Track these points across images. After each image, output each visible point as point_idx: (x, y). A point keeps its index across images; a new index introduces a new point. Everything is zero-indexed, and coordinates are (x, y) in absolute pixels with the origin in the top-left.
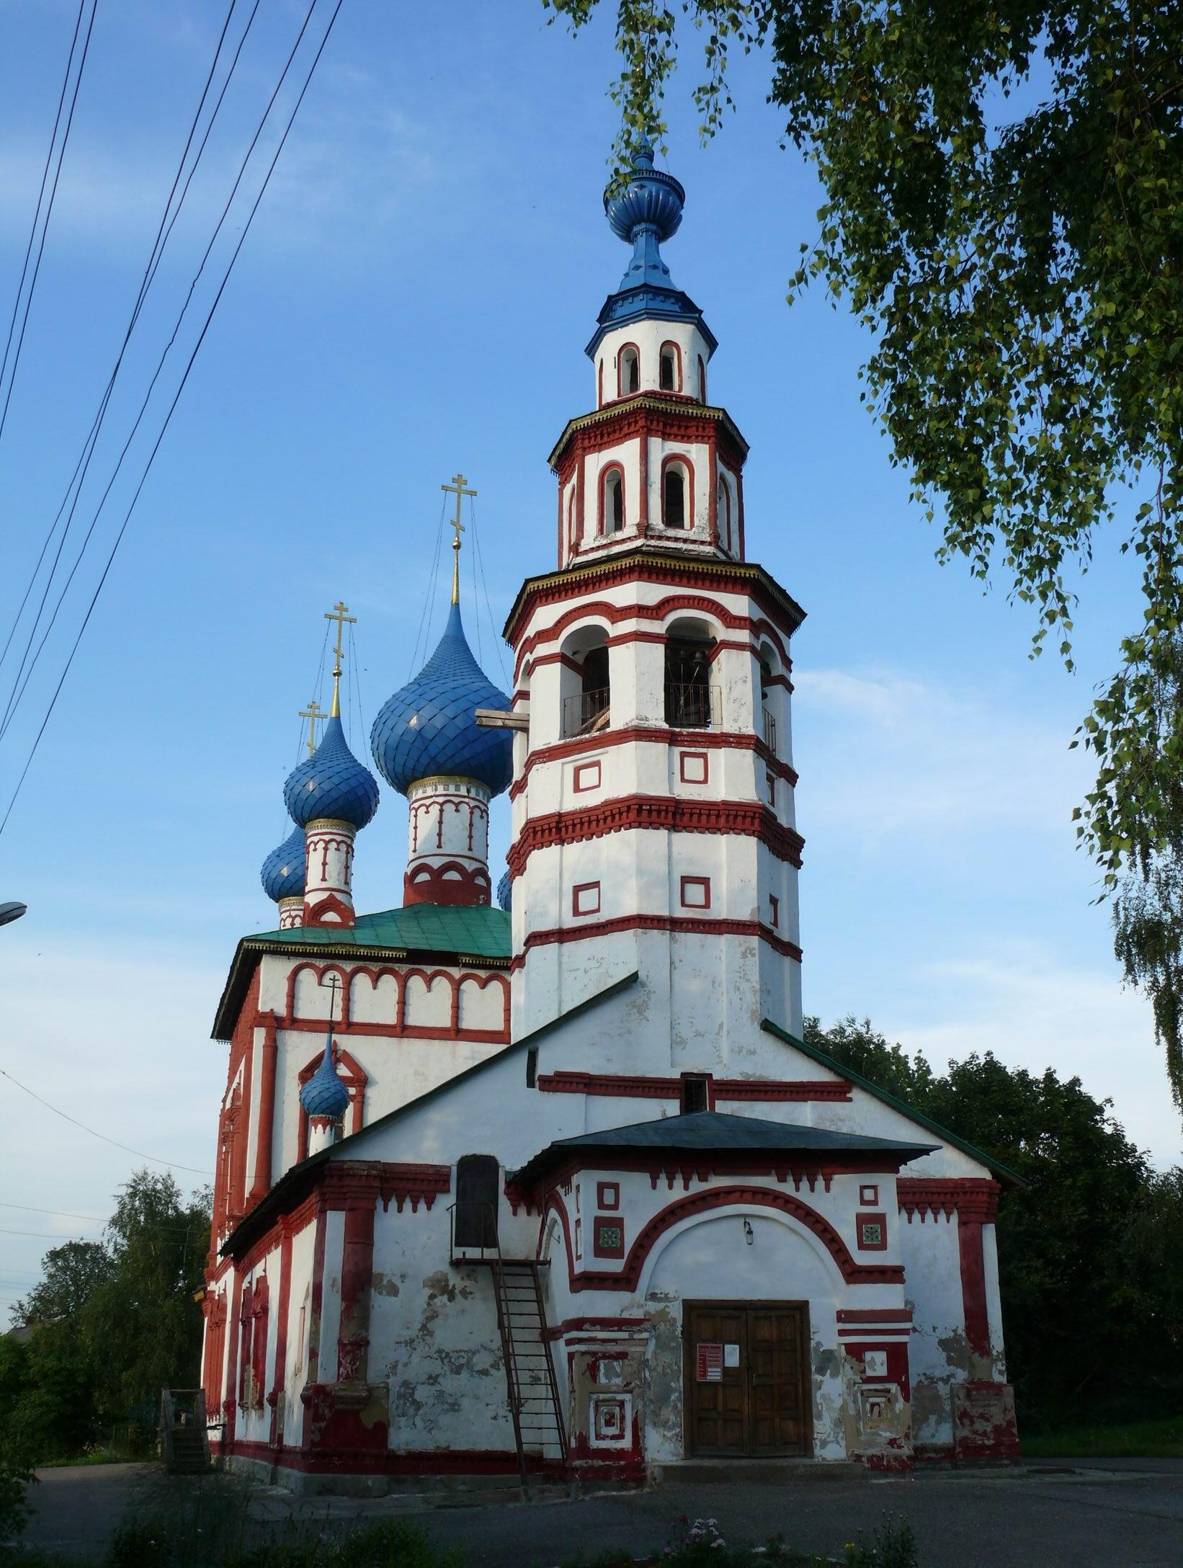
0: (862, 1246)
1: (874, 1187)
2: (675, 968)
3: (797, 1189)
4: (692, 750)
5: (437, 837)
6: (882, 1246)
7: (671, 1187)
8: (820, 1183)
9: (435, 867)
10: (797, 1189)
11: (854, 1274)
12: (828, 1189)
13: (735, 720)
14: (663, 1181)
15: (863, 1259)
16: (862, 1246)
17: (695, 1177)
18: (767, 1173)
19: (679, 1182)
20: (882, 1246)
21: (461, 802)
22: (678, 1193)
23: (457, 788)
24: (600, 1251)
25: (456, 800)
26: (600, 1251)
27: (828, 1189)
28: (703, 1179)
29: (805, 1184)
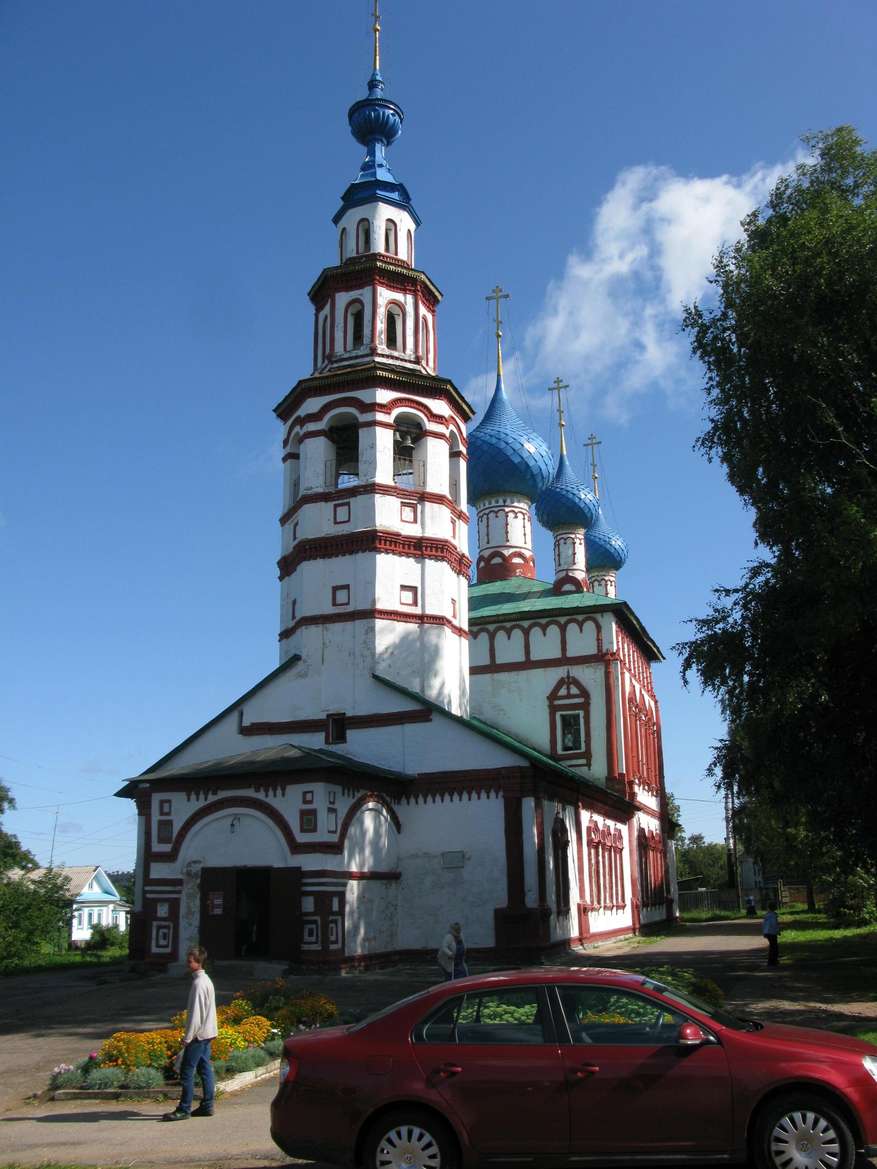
0: (303, 830)
1: (312, 792)
2: (326, 647)
3: (267, 796)
4: (340, 502)
5: (486, 537)
6: (314, 830)
8: (279, 792)
9: (486, 556)
10: (267, 796)
11: (297, 848)
12: (283, 795)
13: (365, 476)
14: (193, 797)
15: (302, 838)
16: (303, 830)
17: (210, 792)
19: (202, 796)
20: (314, 830)
22: (202, 803)
23: (497, 502)
24: (161, 840)
25: (496, 509)
27: (283, 795)
28: (215, 793)
29: (271, 793)
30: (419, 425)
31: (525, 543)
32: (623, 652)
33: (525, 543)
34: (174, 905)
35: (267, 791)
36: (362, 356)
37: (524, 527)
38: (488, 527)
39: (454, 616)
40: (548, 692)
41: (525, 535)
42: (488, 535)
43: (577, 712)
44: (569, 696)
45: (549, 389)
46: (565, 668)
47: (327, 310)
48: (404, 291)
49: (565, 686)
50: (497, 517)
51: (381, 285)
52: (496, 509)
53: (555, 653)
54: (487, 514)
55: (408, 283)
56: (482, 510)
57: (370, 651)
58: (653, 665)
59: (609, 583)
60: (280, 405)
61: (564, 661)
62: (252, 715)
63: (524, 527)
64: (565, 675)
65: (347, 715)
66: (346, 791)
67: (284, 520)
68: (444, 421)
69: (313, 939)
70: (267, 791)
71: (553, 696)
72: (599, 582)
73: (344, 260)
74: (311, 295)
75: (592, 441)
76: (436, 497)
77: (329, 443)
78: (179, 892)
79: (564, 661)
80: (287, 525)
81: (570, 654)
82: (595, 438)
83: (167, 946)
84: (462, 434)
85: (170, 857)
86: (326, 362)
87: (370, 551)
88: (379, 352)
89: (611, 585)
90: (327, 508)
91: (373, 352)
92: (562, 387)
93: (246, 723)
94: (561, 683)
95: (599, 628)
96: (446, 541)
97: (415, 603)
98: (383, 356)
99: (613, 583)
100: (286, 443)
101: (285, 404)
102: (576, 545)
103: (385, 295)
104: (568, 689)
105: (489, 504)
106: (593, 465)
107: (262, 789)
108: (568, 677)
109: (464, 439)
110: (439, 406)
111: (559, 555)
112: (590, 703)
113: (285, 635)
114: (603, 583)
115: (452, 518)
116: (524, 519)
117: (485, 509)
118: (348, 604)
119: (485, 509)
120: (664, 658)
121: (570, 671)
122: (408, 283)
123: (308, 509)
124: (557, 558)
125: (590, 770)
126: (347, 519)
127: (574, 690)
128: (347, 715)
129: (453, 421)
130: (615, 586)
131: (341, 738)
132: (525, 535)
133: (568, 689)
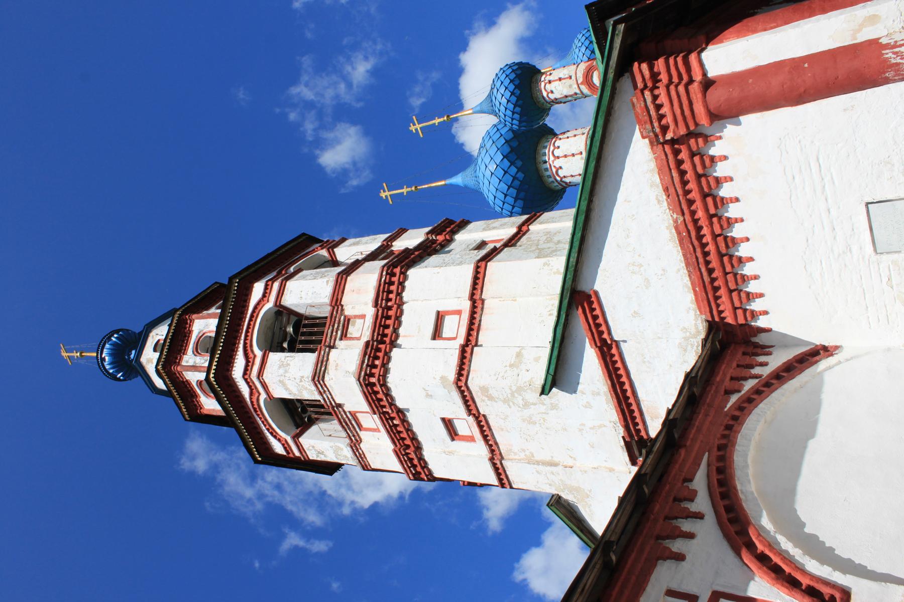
33: (583, 134)
50: (561, 168)
57: (516, 395)
76: (337, 287)
97: (459, 312)
105: (551, 177)
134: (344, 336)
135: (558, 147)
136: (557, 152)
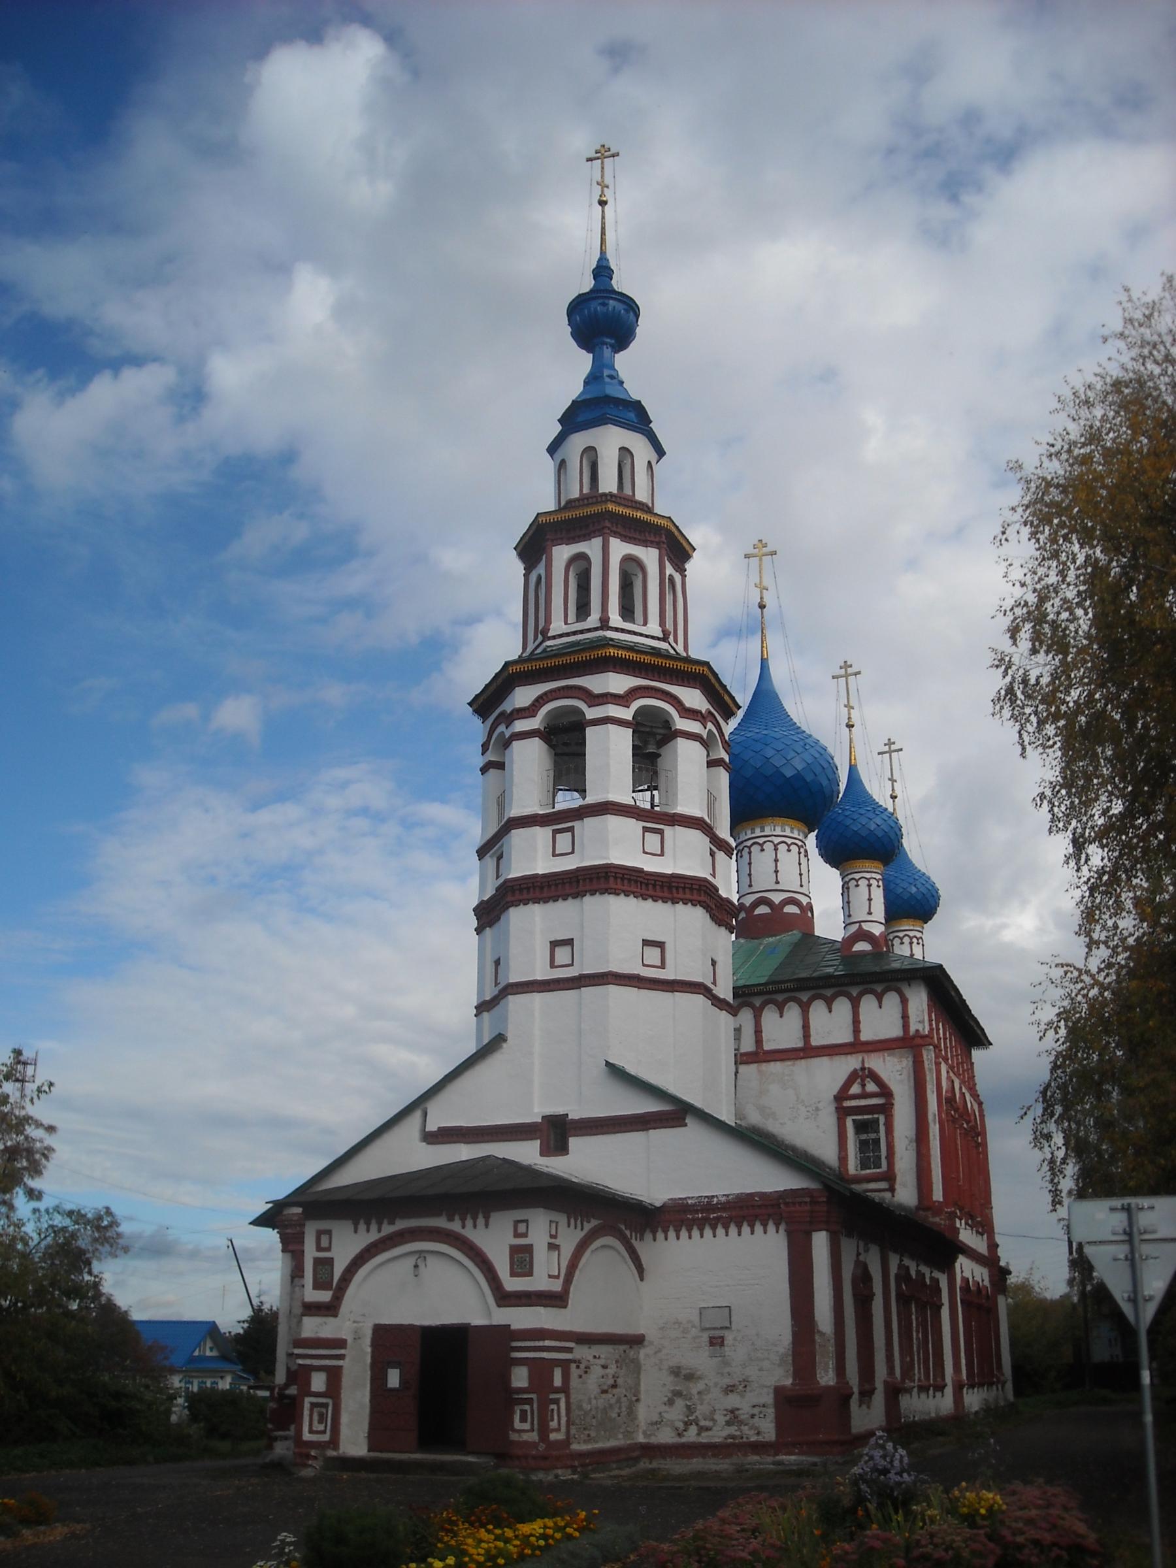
1: (526, 1221)
3: (463, 1227)
7: (368, 1231)
8: (481, 1221)
10: (463, 1227)
11: (505, 1298)
12: (487, 1226)
14: (362, 1227)
15: (512, 1284)
17: (385, 1221)
18: (438, 1214)
21: (765, 842)
22: (373, 1236)
24: (317, 1286)
25: (761, 841)
26: (317, 1286)
27: (487, 1226)
28: (392, 1223)
29: (469, 1222)
30: (667, 723)
31: (801, 886)
32: (938, 1034)
33: (801, 886)
34: (334, 1376)
35: (463, 1220)
36: (589, 630)
37: (800, 864)
38: (750, 864)
39: (714, 983)
40: (835, 1090)
41: (801, 875)
42: (750, 875)
43: (876, 1116)
44: (864, 1095)
45: (833, 677)
46: (860, 1057)
47: (541, 569)
48: (645, 543)
49: (859, 1080)
50: (762, 850)
51: (612, 534)
52: (761, 841)
53: (844, 1036)
54: (749, 847)
55: (650, 532)
56: (742, 842)
58: (977, 1054)
59: (915, 940)
60: (477, 696)
61: (857, 1046)
62: (440, 1116)
63: (800, 864)
64: (858, 1066)
65: (570, 1117)
66: (572, 1221)
67: (482, 853)
68: (699, 718)
69: (527, 1426)
70: (463, 1220)
71: (841, 1096)
72: (901, 939)
73: (563, 504)
74: (519, 549)
75: (890, 748)
77: (544, 746)
78: (342, 1357)
79: (857, 1046)
80: (487, 858)
81: (865, 1036)
82: (894, 743)
83: (324, 1432)
84: (723, 735)
85: (330, 1309)
86: (540, 638)
87: (601, 894)
88: (611, 624)
89: (918, 944)
90: (542, 835)
91: (604, 623)
92: (851, 675)
93: (432, 1127)
94: (853, 1077)
95: (904, 1002)
96: (705, 880)
97: (663, 966)
98: (617, 630)
99: (920, 941)
100: (485, 747)
101: (485, 696)
102: (871, 888)
103: (619, 549)
104: (863, 1086)
106: (892, 780)
107: (457, 1217)
108: (863, 1069)
109: (726, 741)
110: (693, 698)
111: (848, 902)
112: (893, 1104)
113: (483, 1007)
114: (906, 940)
115: (711, 849)
116: (800, 853)
117: (746, 840)
118: (572, 965)
119: (746, 840)
120: (991, 1044)
121: (866, 1060)
122: (650, 532)
123: (518, 836)
124: (846, 904)
125: (893, 1196)
126: (570, 851)
127: (871, 1087)
128: (570, 1117)
129: (711, 718)
130: (923, 945)
131: (561, 1148)
132: (801, 875)
133: (863, 1086)
134: (646, 830)
135: (789, 850)
136: (783, 847)
